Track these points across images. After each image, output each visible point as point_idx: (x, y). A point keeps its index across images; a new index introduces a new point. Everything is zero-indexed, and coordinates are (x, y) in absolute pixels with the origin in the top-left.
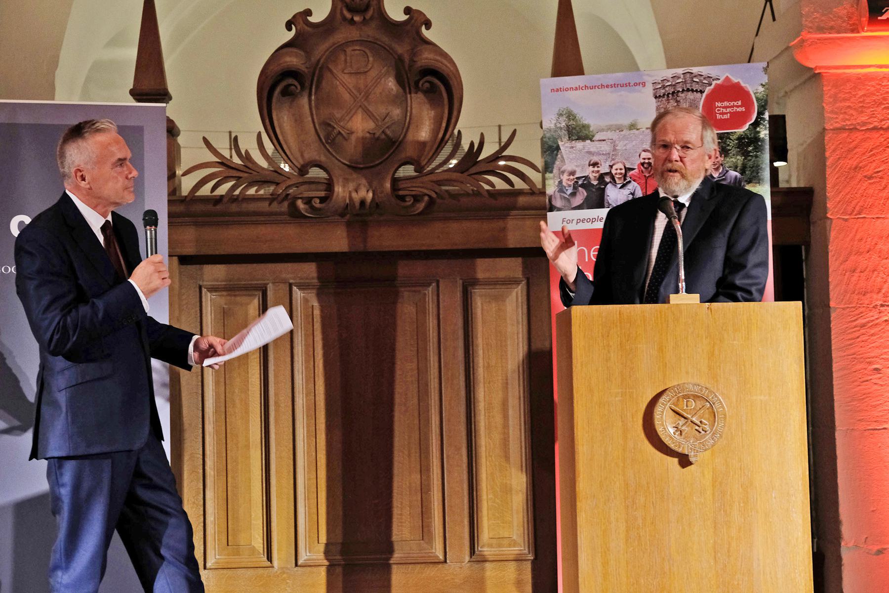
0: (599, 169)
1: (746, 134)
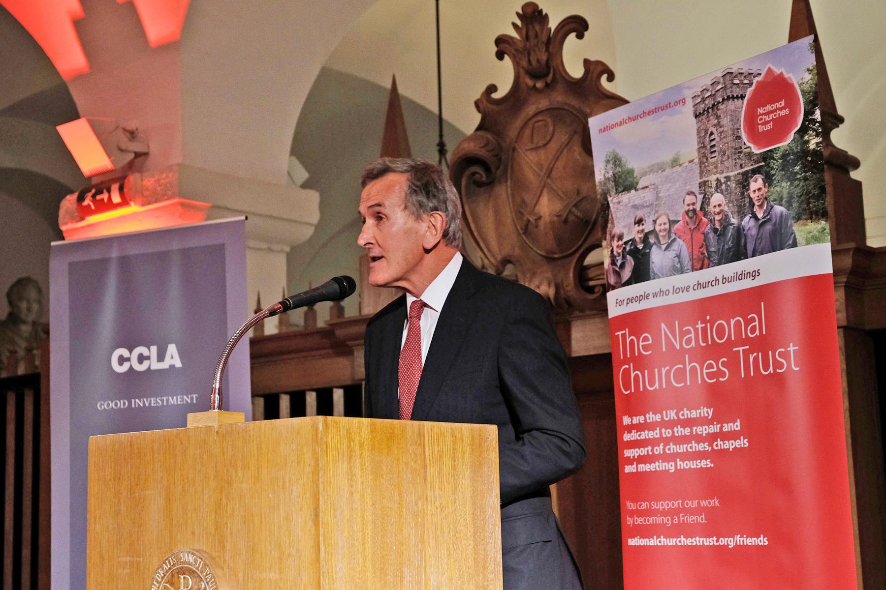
0: (643, 227)
1: (791, 149)
